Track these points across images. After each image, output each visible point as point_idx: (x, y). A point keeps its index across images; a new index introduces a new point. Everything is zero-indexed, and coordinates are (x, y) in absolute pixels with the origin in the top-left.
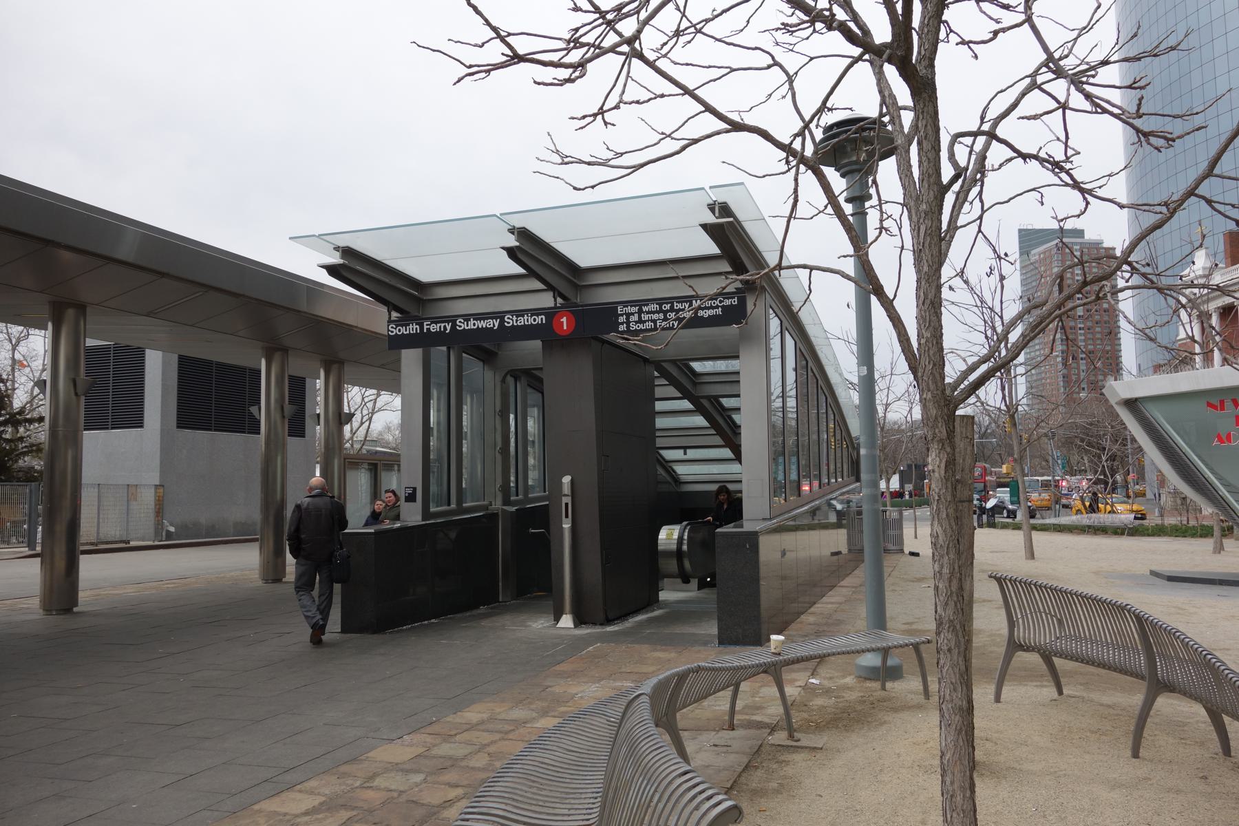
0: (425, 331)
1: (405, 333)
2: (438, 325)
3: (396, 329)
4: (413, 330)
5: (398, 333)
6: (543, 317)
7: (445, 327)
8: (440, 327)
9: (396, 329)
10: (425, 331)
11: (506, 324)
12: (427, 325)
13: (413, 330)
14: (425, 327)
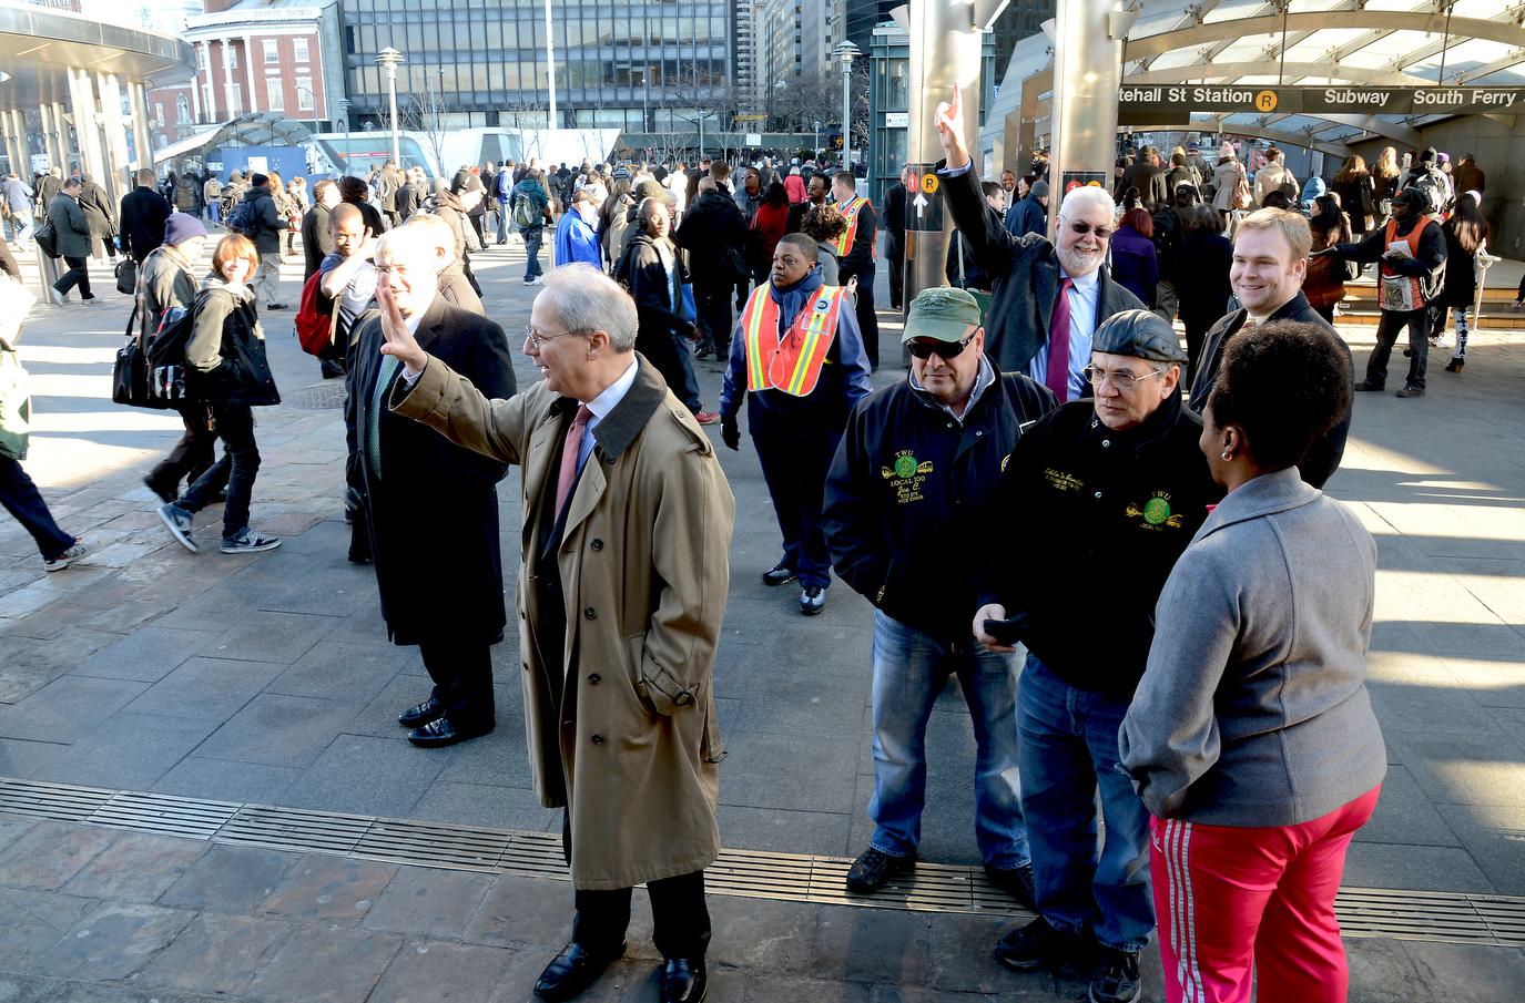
0: (1474, 102)
1: (1439, 102)
3: (1425, 96)
4: (1452, 100)
5: (1428, 102)
8: (1498, 98)
9: (1425, 96)
10: (1474, 102)
12: (1478, 94)
13: (1452, 100)
14: (1475, 97)
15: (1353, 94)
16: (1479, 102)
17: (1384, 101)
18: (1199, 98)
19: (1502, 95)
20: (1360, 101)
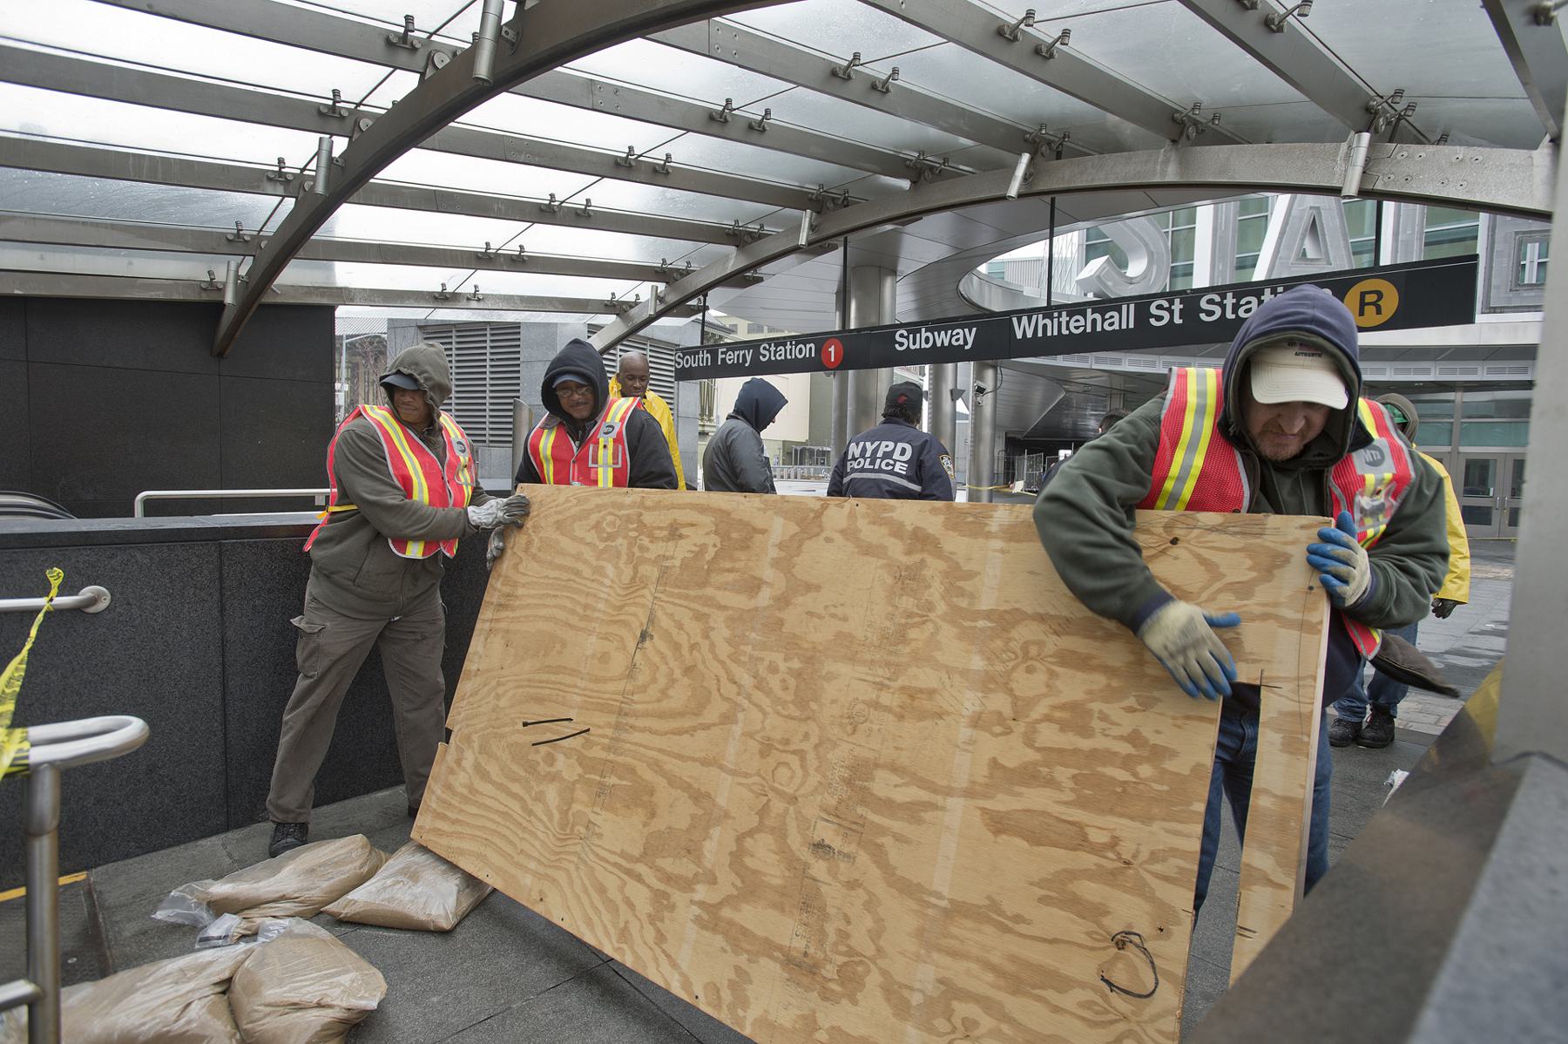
2: (736, 353)
6: (812, 345)
7: (744, 355)
9: (683, 359)
11: (1153, 321)
12: (722, 353)
14: (720, 356)
15: (929, 334)
16: (723, 360)
17: (970, 340)
18: (1159, 318)
19: (742, 353)
20: (939, 345)
